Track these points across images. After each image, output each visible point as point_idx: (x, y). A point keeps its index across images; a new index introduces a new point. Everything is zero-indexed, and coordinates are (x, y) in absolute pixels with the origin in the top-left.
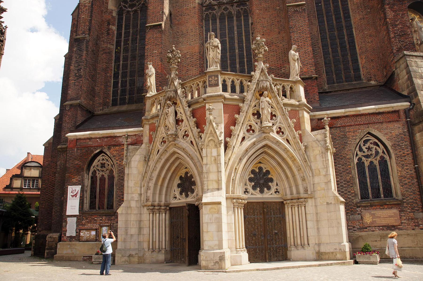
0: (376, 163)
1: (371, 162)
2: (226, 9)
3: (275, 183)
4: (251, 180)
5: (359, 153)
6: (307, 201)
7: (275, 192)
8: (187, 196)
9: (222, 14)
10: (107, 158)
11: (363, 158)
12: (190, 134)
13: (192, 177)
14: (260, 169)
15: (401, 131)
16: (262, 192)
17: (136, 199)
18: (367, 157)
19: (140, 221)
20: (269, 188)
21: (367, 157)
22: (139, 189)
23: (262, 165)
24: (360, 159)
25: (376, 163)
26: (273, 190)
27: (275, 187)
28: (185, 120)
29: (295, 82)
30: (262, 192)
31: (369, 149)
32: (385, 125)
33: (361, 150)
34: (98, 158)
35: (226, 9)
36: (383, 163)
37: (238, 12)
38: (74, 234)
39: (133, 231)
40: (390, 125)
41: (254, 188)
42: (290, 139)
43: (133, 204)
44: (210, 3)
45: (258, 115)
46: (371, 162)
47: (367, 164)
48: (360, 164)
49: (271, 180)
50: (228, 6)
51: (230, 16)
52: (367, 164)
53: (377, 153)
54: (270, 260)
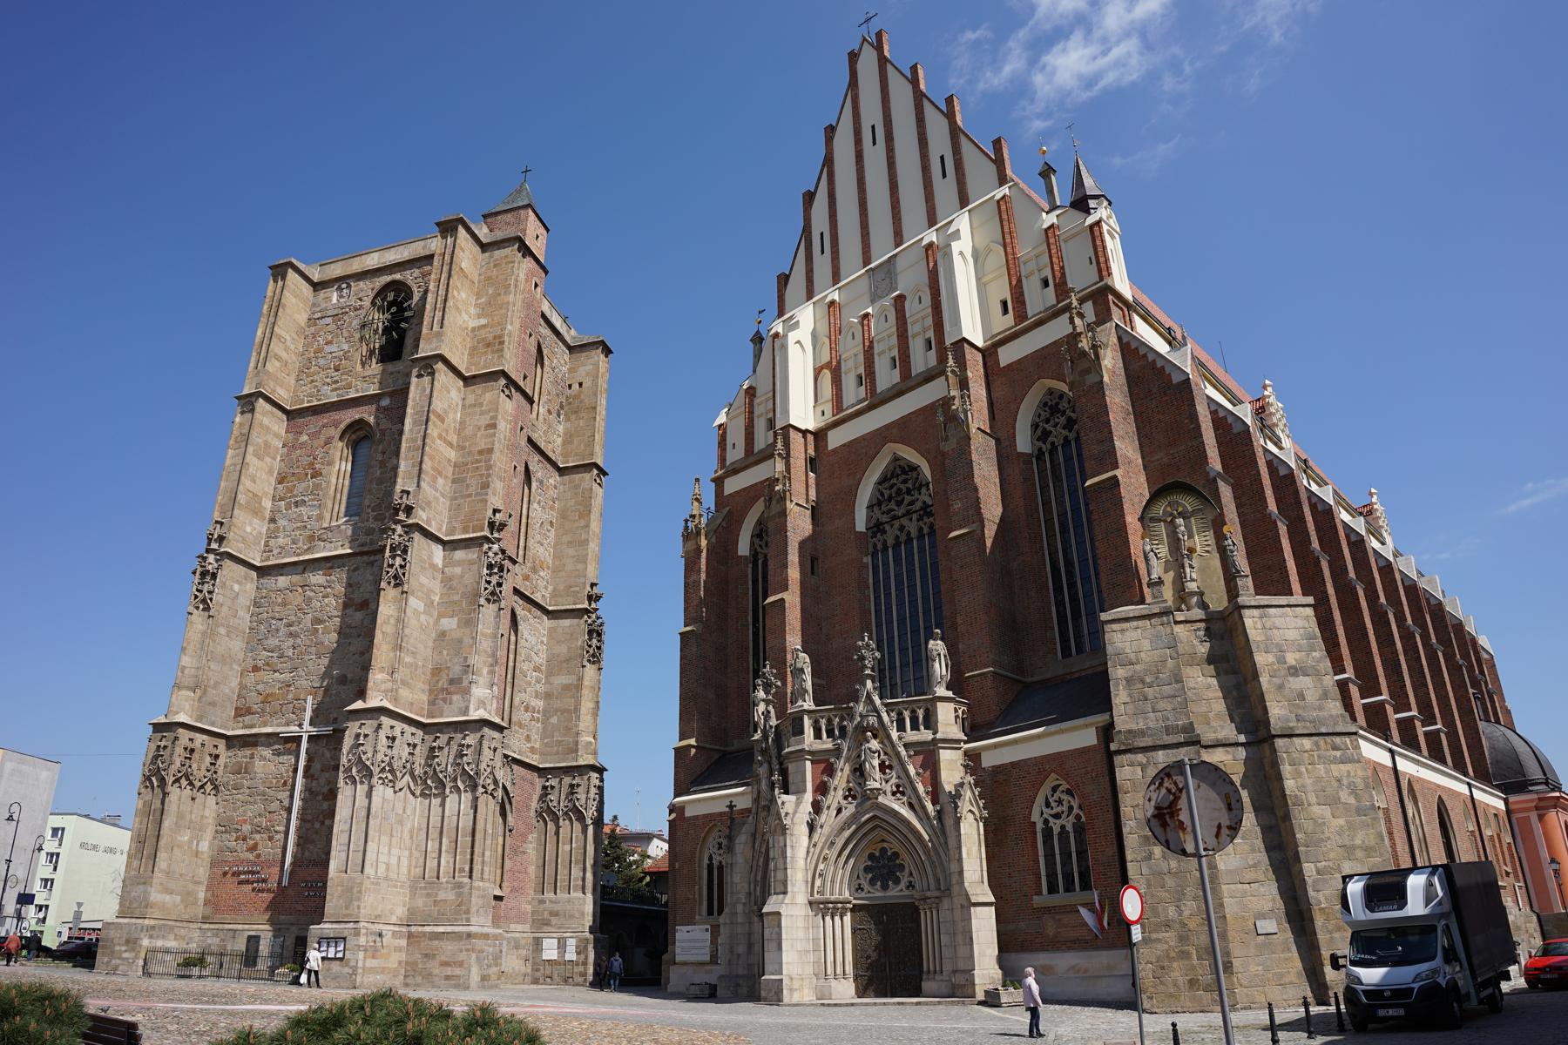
0: (1069, 828)
1: (1063, 827)
3: (906, 872)
4: (867, 869)
5: (1045, 810)
6: (941, 901)
7: (908, 887)
9: (897, 537)
11: (1051, 819)
16: (885, 887)
17: (743, 901)
18: (1057, 816)
19: (750, 934)
20: (897, 881)
21: (1057, 816)
22: (746, 885)
23: (885, 845)
24: (1046, 822)
25: (1069, 828)
26: (903, 885)
27: (906, 879)
30: (885, 887)
31: (1060, 802)
33: (1048, 805)
35: (902, 528)
37: (921, 529)
39: (741, 949)
41: (872, 882)
42: (914, 801)
43: (740, 908)
45: (859, 771)
46: (1063, 827)
47: (1056, 830)
48: (1048, 832)
49: (902, 868)
52: (1056, 830)
54: (893, 996)
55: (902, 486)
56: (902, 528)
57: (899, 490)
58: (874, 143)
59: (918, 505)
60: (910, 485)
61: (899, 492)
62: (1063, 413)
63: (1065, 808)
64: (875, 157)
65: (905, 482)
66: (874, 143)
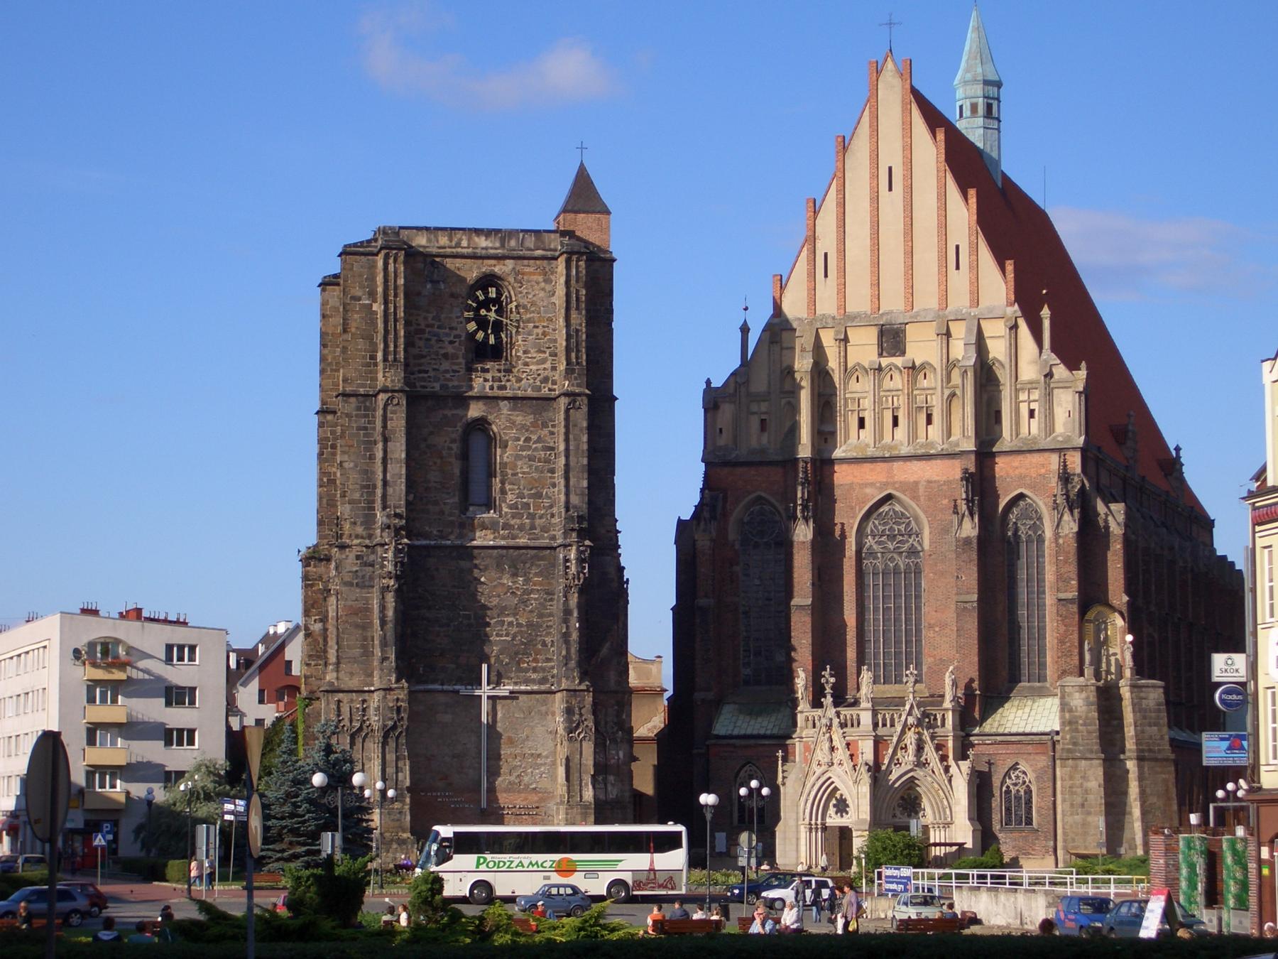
1: (1018, 791)
2: (892, 559)
8: (842, 816)
10: (755, 768)
12: (845, 764)
13: (845, 800)
14: (909, 795)
15: (1045, 764)
18: (1015, 785)
21: (1015, 785)
24: (1008, 787)
28: (840, 750)
29: (947, 710)
31: (1017, 777)
32: (1032, 757)
34: (745, 769)
36: (1029, 792)
38: (724, 850)
40: (1037, 757)
44: (871, 546)
46: (1018, 791)
50: (896, 556)
51: (896, 571)
53: (1024, 782)
55: (896, 527)
56: (892, 559)
57: (891, 529)
58: (890, 189)
59: (906, 546)
60: (902, 527)
61: (891, 529)
62: (1031, 519)
63: (1021, 781)
64: (892, 203)
65: (899, 524)
66: (890, 189)
